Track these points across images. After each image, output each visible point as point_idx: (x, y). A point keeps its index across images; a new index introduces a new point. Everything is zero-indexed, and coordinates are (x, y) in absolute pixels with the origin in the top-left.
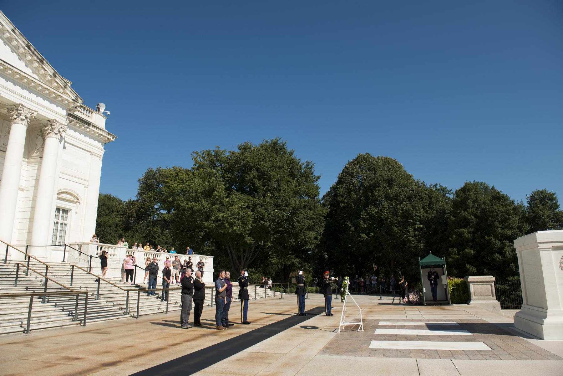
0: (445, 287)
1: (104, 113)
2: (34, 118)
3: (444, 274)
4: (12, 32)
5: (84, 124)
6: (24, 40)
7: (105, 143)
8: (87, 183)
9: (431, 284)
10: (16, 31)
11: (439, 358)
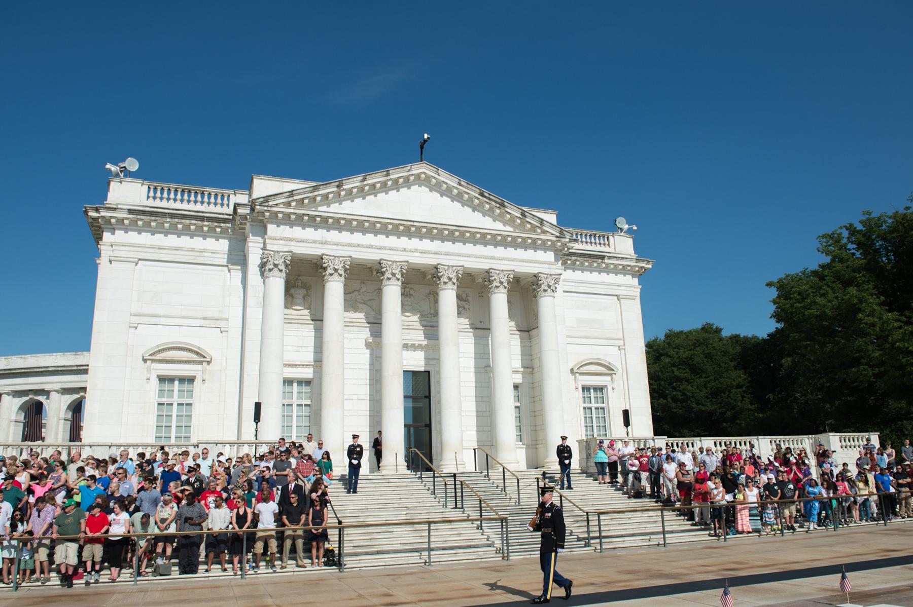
1: (630, 232)
2: (511, 280)
4: (458, 187)
5: (595, 260)
6: (474, 188)
7: (640, 275)
8: (621, 343)
10: (462, 183)
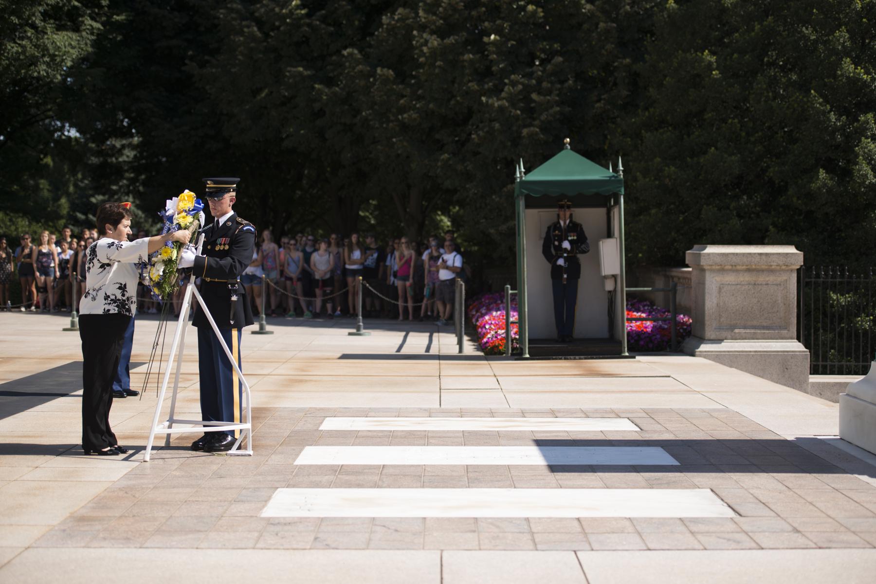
0: (609, 286)
3: (609, 235)
9: (556, 272)
11: (532, 547)
